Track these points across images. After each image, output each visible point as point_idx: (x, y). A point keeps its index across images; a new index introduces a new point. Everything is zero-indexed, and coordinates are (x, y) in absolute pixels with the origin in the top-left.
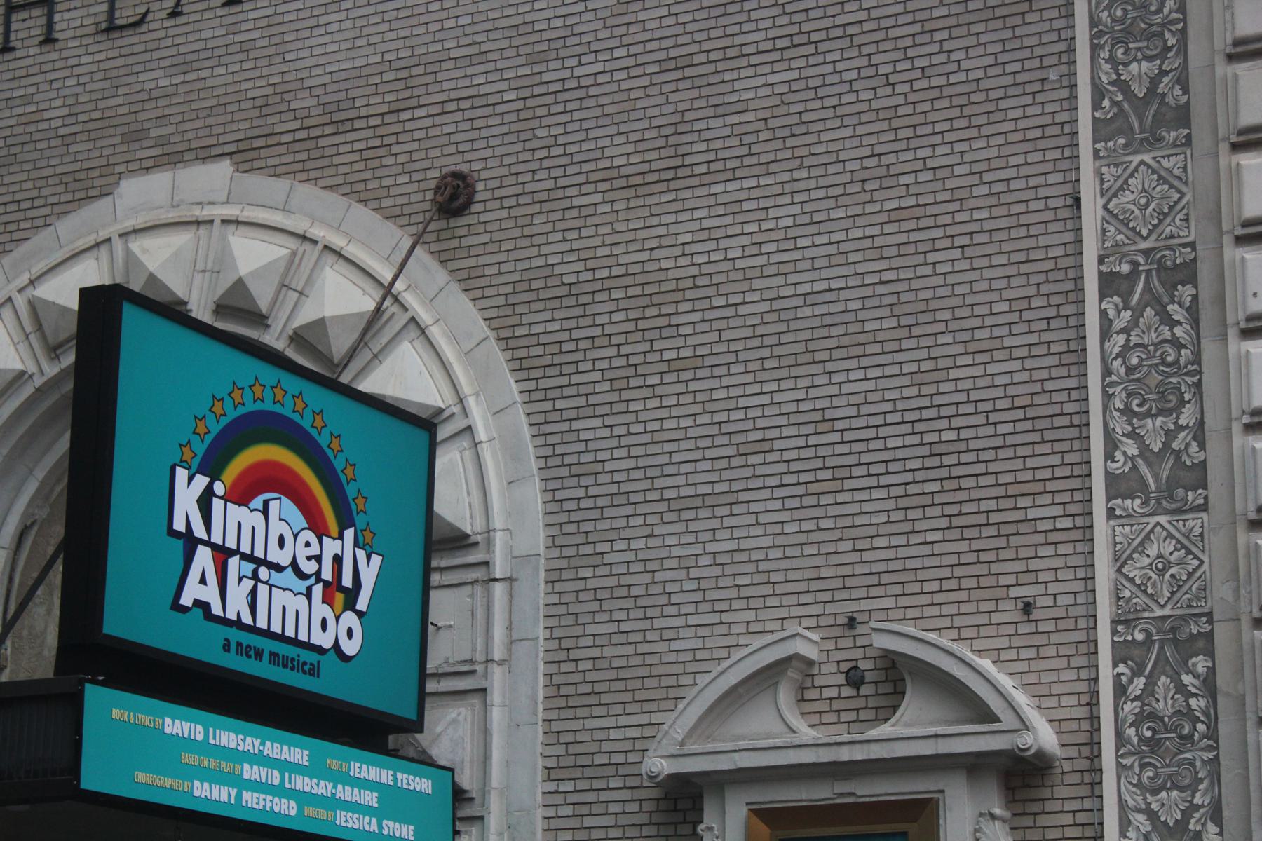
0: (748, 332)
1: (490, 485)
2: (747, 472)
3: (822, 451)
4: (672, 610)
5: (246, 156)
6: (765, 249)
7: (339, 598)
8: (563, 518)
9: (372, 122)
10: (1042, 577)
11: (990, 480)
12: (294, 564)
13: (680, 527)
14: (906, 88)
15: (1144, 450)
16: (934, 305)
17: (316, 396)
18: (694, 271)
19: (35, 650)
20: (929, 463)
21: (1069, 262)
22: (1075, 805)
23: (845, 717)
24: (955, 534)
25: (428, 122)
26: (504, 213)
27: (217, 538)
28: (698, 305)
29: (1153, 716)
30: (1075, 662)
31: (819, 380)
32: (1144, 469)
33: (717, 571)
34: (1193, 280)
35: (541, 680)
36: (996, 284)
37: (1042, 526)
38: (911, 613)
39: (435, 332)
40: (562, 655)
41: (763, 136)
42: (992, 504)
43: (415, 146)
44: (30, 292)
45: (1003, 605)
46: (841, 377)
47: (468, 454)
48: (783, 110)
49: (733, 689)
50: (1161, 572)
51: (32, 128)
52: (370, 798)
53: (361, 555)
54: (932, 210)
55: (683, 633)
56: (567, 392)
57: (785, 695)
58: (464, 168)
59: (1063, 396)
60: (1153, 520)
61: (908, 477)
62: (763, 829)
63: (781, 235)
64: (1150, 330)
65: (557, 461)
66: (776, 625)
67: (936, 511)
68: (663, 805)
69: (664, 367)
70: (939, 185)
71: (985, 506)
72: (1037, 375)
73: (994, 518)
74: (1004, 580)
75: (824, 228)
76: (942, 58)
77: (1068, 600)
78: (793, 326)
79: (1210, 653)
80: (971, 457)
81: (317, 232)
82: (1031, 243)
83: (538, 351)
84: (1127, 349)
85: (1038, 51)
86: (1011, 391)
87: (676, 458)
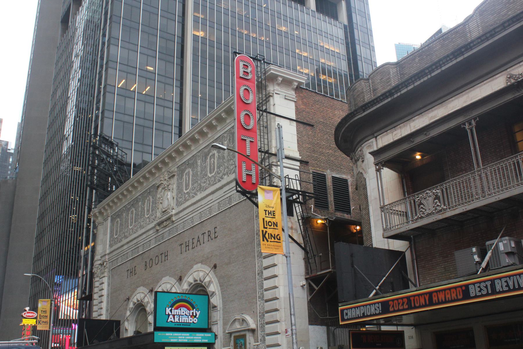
5: (202, 262)
27: (173, 314)
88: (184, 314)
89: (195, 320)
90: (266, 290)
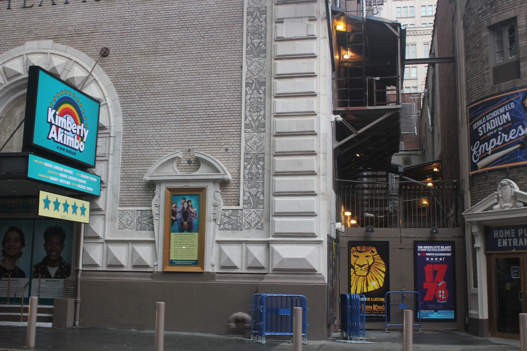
0: (170, 88)
1: (111, 116)
2: (168, 118)
3: (185, 114)
4: (151, 146)
5: (56, 39)
6: (175, 70)
7: (80, 138)
8: (127, 124)
9: (86, 34)
10: (230, 144)
11: (220, 123)
12: (72, 130)
13: (153, 128)
14: (207, 39)
15: (253, 119)
16: (210, 85)
17: (78, 94)
18: (159, 74)
19: (16, 145)
20: (208, 118)
21: (239, 79)
22: (234, 190)
23: (187, 170)
24: (212, 134)
25: (99, 36)
26: (116, 57)
27: (56, 124)
28: (159, 81)
29: (251, 173)
30: (236, 161)
31: (185, 99)
32: (252, 123)
33: (161, 138)
34: (265, 85)
35: (121, 159)
36: (224, 82)
37: (231, 133)
38: (202, 149)
39: (99, 82)
40: (125, 154)
41: (175, 46)
42: (221, 128)
43: (96, 41)
44: (3, 65)
45: (222, 149)
46: (190, 99)
47: (106, 109)
48: (180, 41)
49: (164, 163)
50: (255, 144)
51: (4, 28)
52: (84, 182)
53: (85, 129)
54: (211, 66)
55: (153, 151)
56: (129, 97)
57: (175, 165)
58: (107, 47)
59: (237, 107)
60: (254, 133)
61: (203, 121)
62: (169, 192)
63: (178, 68)
64: (255, 95)
65: (126, 112)
66: (173, 150)
67: (209, 129)
68: (147, 186)
69: (151, 94)
70: (213, 61)
71: (219, 128)
72: (231, 102)
73: (221, 131)
74: (222, 144)
75: (188, 67)
76: (215, 34)
77: (235, 149)
78: (180, 87)
79: (264, 161)
80: (217, 118)
81: (72, 58)
82: (232, 74)
83: (123, 88)
84: (250, 98)
85: (235, 35)
86: (226, 105)
87: (153, 113)
90: (279, 115)
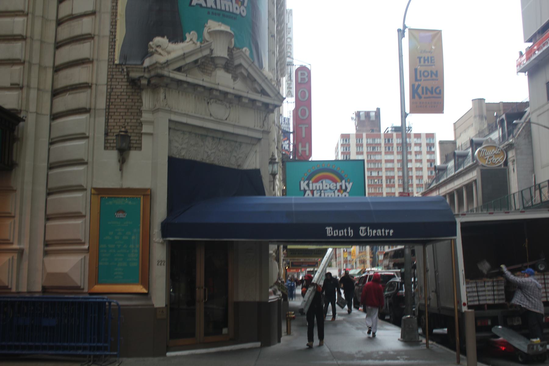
7: (342, 191)
12: (330, 188)
88: (328, 187)
89: (344, 195)
